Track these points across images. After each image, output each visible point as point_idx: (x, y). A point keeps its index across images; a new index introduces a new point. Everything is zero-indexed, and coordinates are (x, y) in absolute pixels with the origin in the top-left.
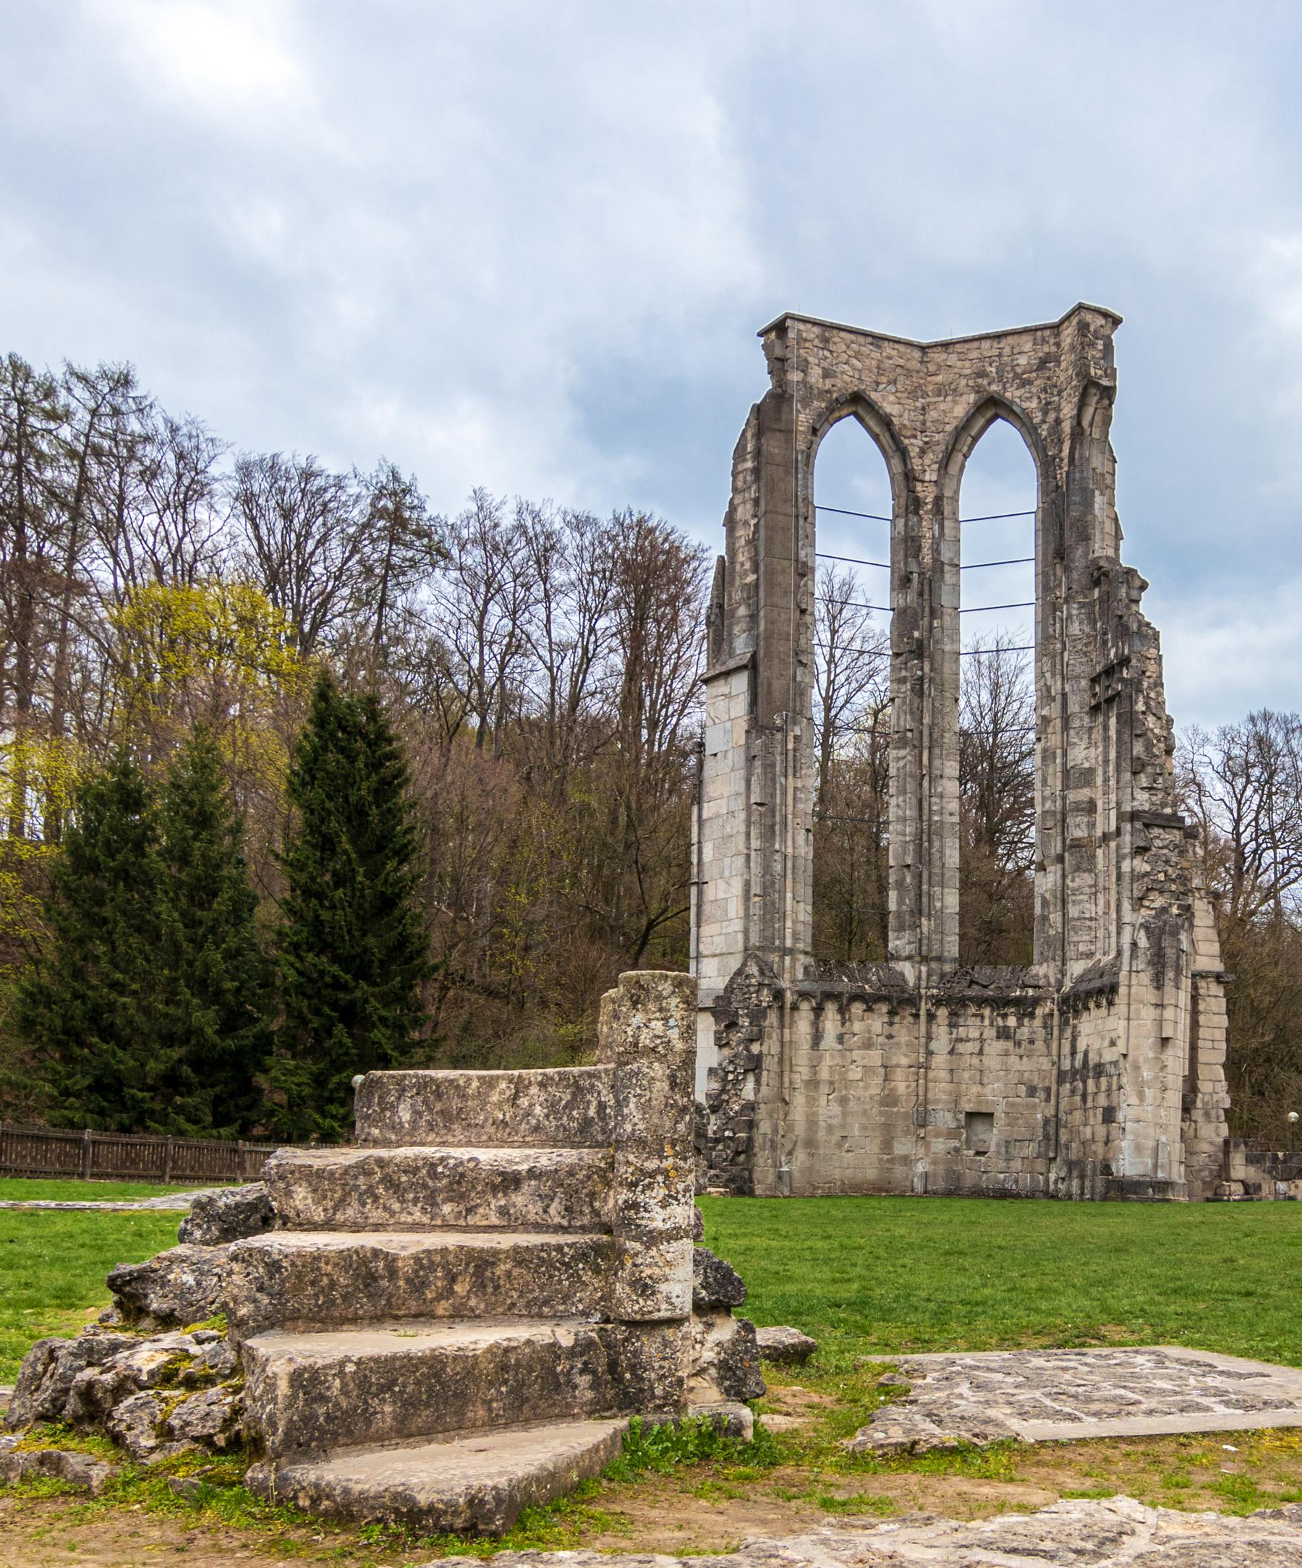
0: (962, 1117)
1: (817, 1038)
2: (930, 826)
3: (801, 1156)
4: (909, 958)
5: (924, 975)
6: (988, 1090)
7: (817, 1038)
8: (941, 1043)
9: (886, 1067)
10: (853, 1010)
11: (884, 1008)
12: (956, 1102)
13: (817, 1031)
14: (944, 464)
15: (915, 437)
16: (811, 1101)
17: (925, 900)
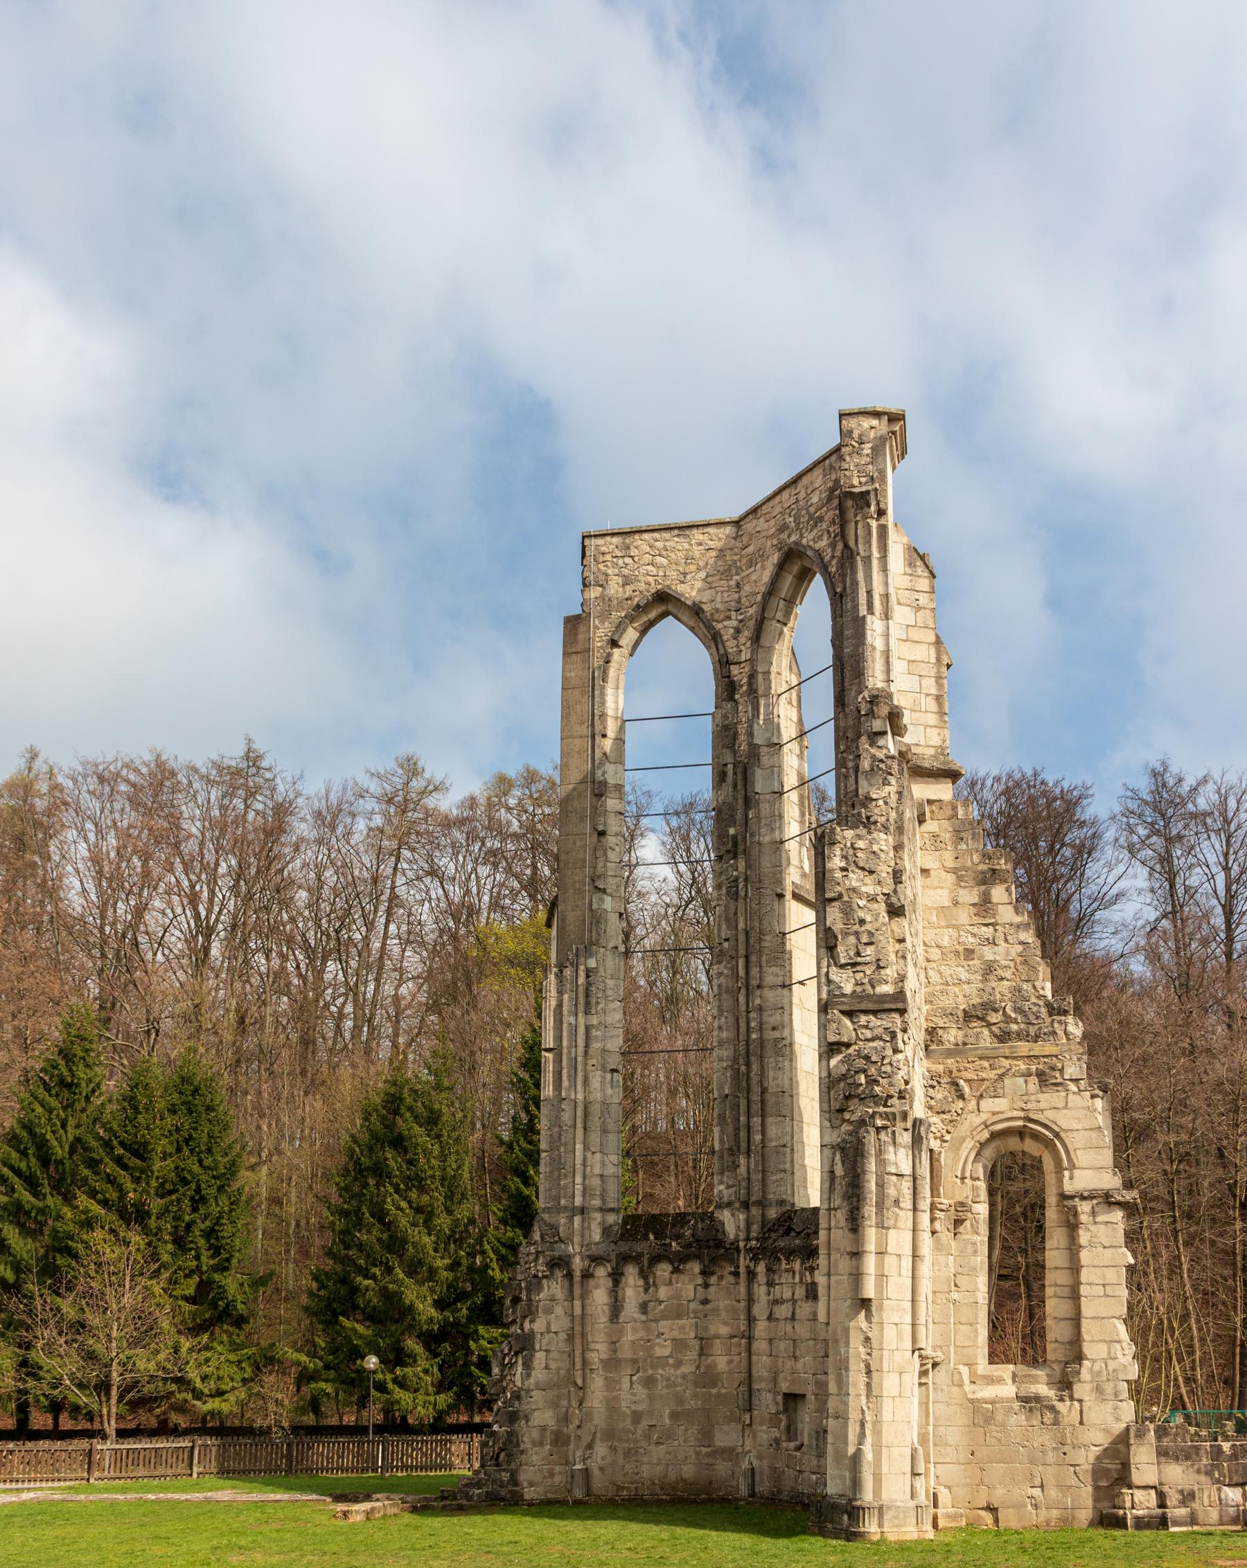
0: (780, 1398)
1: (616, 1308)
2: (748, 1045)
3: (601, 1450)
4: (729, 1204)
5: (742, 1225)
6: (799, 1366)
7: (616, 1308)
8: (760, 1310)
9: (702, 1339)
10: (658, 1273)
11: (696, 1267)
12: (775, 1380)
13: (616, 1300)
14: (756, 638)
15: (729, 618)
16: (611, 1384)
17: (743, 1134)
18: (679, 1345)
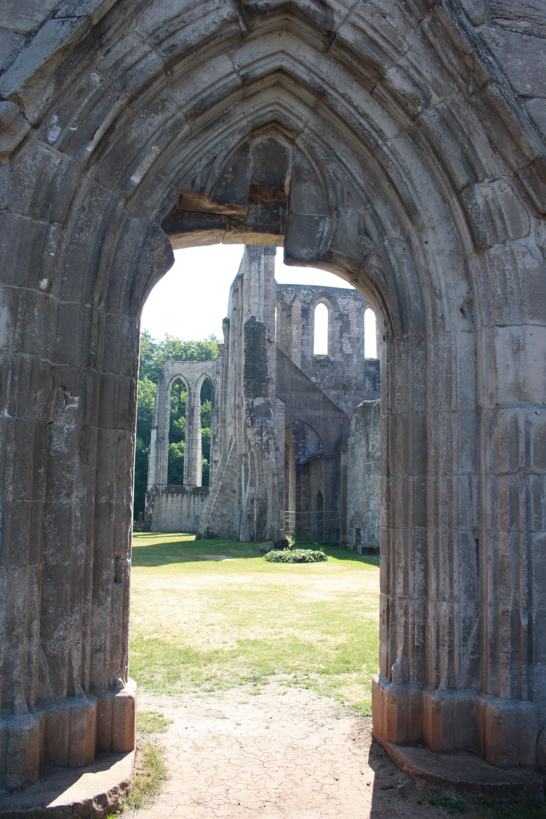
7: (167, 501)
8: (192, 503)
11: (180, 495)
18: (177, 508)
